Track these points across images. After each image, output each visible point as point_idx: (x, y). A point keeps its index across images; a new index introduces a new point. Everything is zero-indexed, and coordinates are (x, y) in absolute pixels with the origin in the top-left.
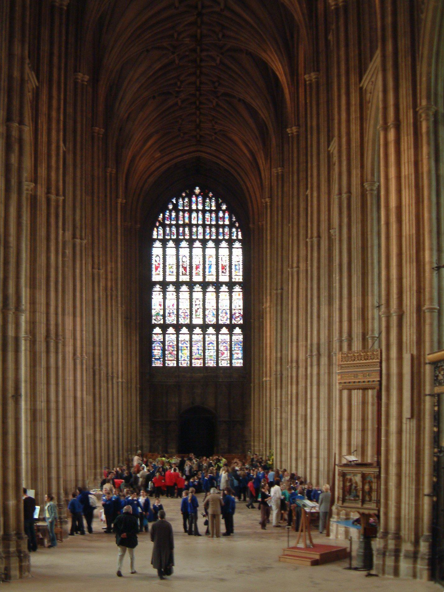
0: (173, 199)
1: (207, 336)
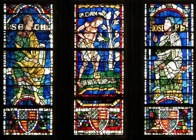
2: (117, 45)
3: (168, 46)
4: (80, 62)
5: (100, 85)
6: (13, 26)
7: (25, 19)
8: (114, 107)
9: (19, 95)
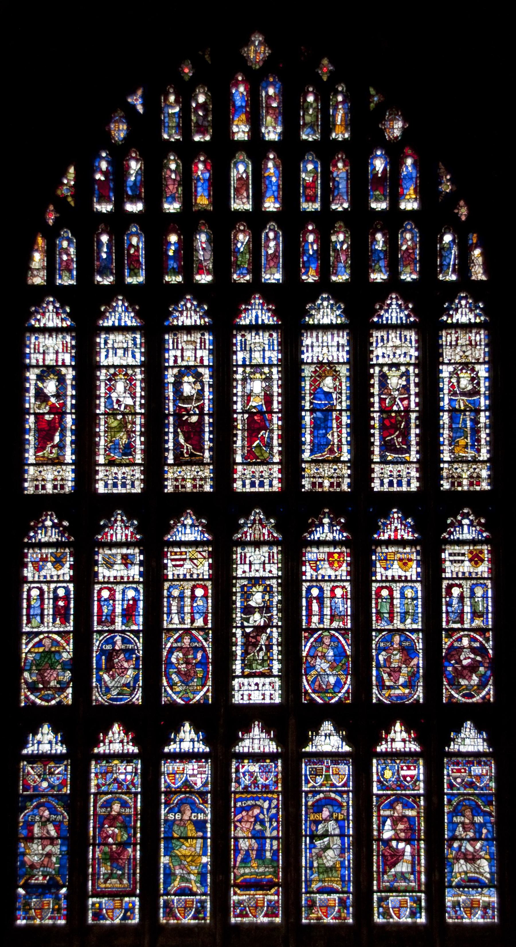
0: (133, 92)
1: (305, 769)
2: (275, 833)
4: (237, 850)
6: (171, 816)
7: (182, 809)
8: (272, 895)
9: (176, 883)
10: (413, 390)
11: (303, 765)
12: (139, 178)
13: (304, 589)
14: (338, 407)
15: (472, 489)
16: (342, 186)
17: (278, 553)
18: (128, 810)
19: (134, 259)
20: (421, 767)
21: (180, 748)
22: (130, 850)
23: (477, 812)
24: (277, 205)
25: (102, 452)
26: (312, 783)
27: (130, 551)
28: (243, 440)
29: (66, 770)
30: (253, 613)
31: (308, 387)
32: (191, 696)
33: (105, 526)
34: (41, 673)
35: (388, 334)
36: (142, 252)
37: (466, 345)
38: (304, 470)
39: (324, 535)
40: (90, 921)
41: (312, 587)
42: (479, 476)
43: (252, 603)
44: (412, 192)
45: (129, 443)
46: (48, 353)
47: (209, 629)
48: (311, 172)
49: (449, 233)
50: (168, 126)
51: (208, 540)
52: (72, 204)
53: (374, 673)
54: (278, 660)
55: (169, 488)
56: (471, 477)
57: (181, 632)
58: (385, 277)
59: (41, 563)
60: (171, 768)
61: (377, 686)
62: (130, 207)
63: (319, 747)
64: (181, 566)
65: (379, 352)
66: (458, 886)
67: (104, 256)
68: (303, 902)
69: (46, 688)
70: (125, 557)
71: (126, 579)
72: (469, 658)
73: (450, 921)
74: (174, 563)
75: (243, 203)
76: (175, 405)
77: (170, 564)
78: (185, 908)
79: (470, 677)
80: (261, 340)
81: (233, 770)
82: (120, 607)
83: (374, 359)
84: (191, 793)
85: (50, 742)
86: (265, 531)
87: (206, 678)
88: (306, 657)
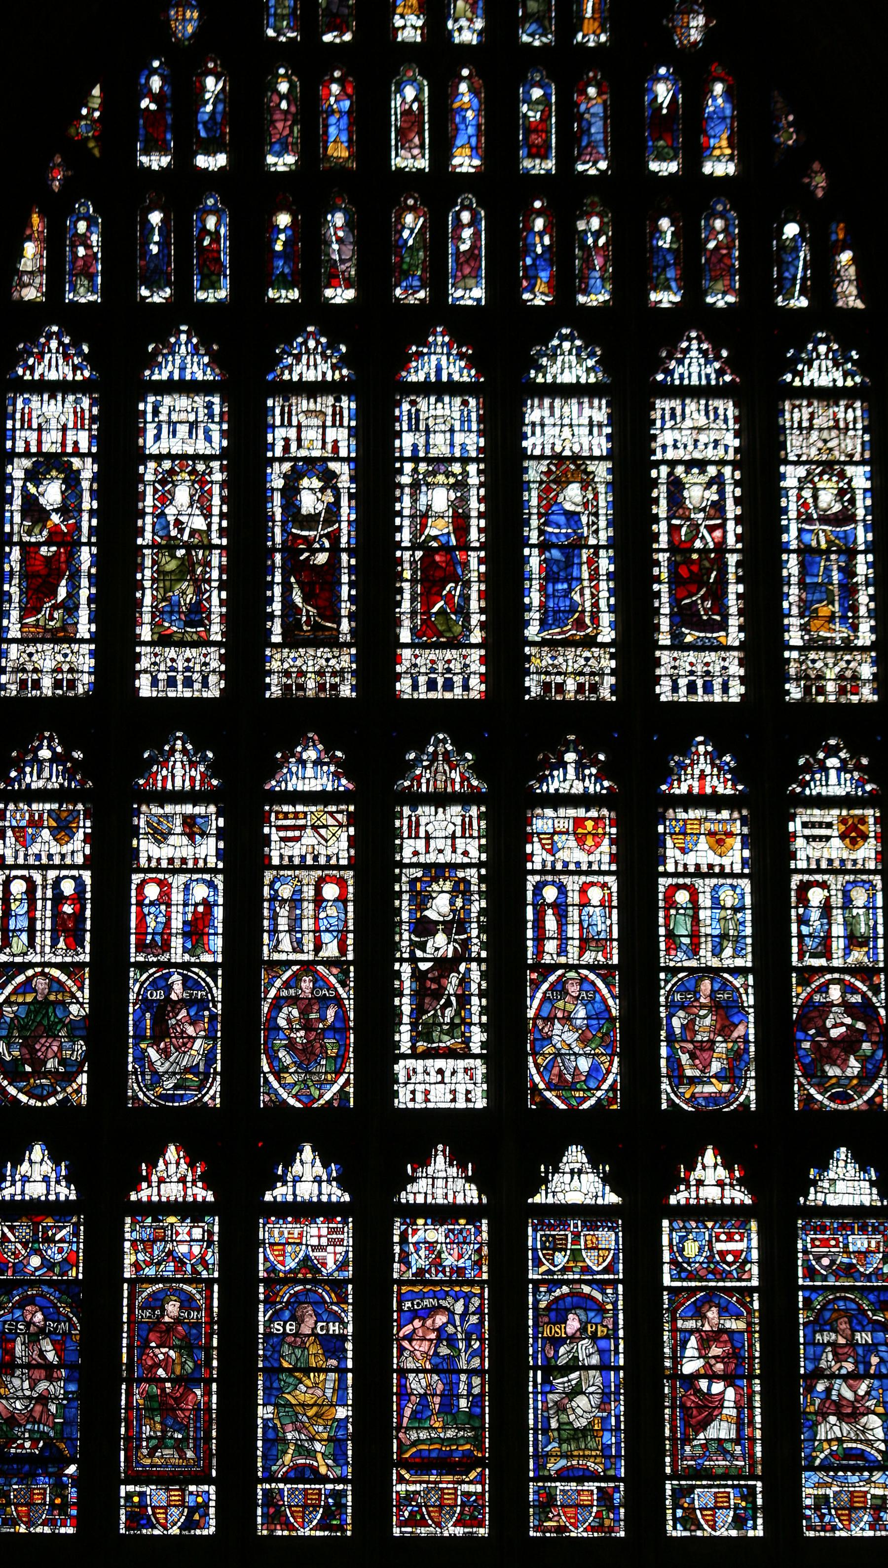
1: (533, 1238)
2: (476, 1363)
3: (574, 1365)
4: (404, 1394)
5: (443, 1440)
6: (277, 1327)
8: (470, 1482)
9: (287, 1458)
10: (732, 510)
11: (530, 1229)
12: (220, 107)
13: (530, 887)
14: (592, 541)
15: (843, 700)
16: (596, 129)
17: (479, 818)
18: (194, 1314)
19: (210, 258)
20: (754, 1236)
21: (294, 1194)
22: (198, 1392)
23: (860, 1323)
24: (477, 162)
25: (147, 618)
26: (546, 1266)
27: (200, 810)
28: (413, 600)
29: (76, 1234)
30: (434, 934)
31: (534, 502)
32: (316, 1094)
33: (152, 761)
34: (28, 1045)
35: (684, 406)
36: (225, 244)
37: (829, 429)
38: (528, 658)
39: (567, 785)
40: (122, 1531)
41: (545, 884)
42: (856, 677)
43: (431, 914)
44: (724, 143)
45: (199, 602)
46: (48, 430)
47: (349, 963)
48: (538, 102)
49: (793, 220)
50: (275, 14)
51: (347, 790)
52: (96, 152)
53: (664, 1052)
54: (481, 1024)
55: (273, 689)
56: (841, 677)
57: (295, 968)
58: (677, 299)
59: (30, 831)
60: (276, 1235)
61: (668, 1076)
62: (202, 161)
63: (560, 1196)
64: (297, 839)
65: (667, 437)
66: (825, 1467)
67: (155, 249)
68: (531, 1498)
69: (38, 1072)
70: (189, 822)
71: (190, 865)
72: (842, 1024)
73: (811, 1534)
74: (282, 834)
75: (414, 157)
76: (283, 531)
77: (274, 837)
78: (305, 1506)
79: (846, 1060)
80: (447, 412)
81: (396, 1239)
82: (180, 917)
83: (659, 451)
84: (315, 1282)
85: (46, 1179)
86: (455, 775)
87: (344, 1058)
88: (534, 1019)
